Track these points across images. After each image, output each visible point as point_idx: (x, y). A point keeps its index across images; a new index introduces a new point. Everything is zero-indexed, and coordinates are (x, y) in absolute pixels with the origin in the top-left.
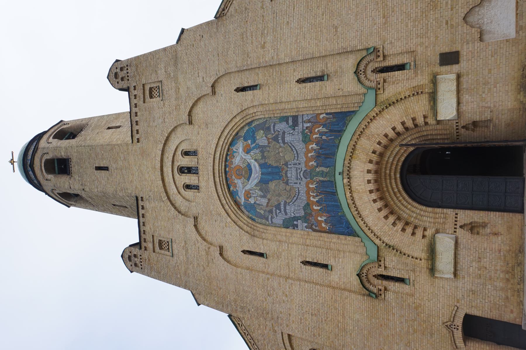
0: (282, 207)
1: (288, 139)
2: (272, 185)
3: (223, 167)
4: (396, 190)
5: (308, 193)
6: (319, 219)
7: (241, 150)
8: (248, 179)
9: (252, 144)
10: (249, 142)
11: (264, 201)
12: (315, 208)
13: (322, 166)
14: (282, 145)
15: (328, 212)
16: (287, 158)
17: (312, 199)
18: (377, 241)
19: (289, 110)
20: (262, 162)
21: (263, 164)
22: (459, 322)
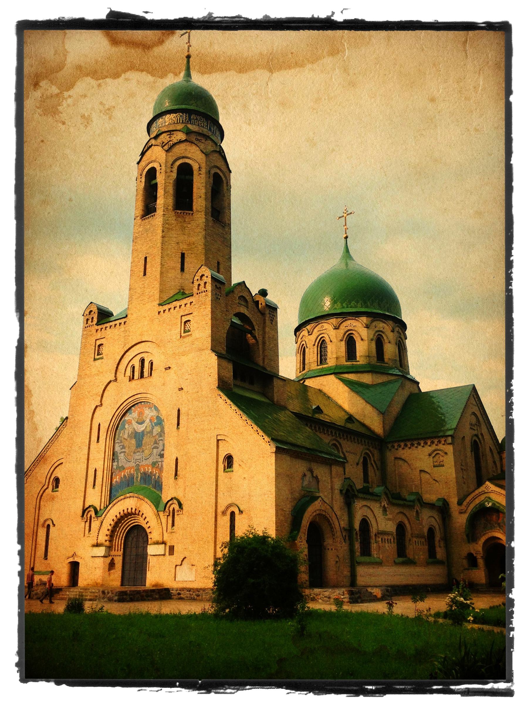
0: (123, 450)
1: (155, 451)
2: (133, 441)
3: (143, 401)
4: (130, 523)
5: (130, 468)
6: (118, 477)
7: (152, 414)
8: (137, 422)
9: (154, 423)
10: (156, 421)
11: (126, 436)
12: (123, 473)
13: (141, 478)
14: (152, 447)
15: (120, 482)
16: (145, 452)
17: (127, 471)
18: (103, 516)
19: (166, 453)
20: (145, 433)
21: (144, 434)
22: (76, 559)
